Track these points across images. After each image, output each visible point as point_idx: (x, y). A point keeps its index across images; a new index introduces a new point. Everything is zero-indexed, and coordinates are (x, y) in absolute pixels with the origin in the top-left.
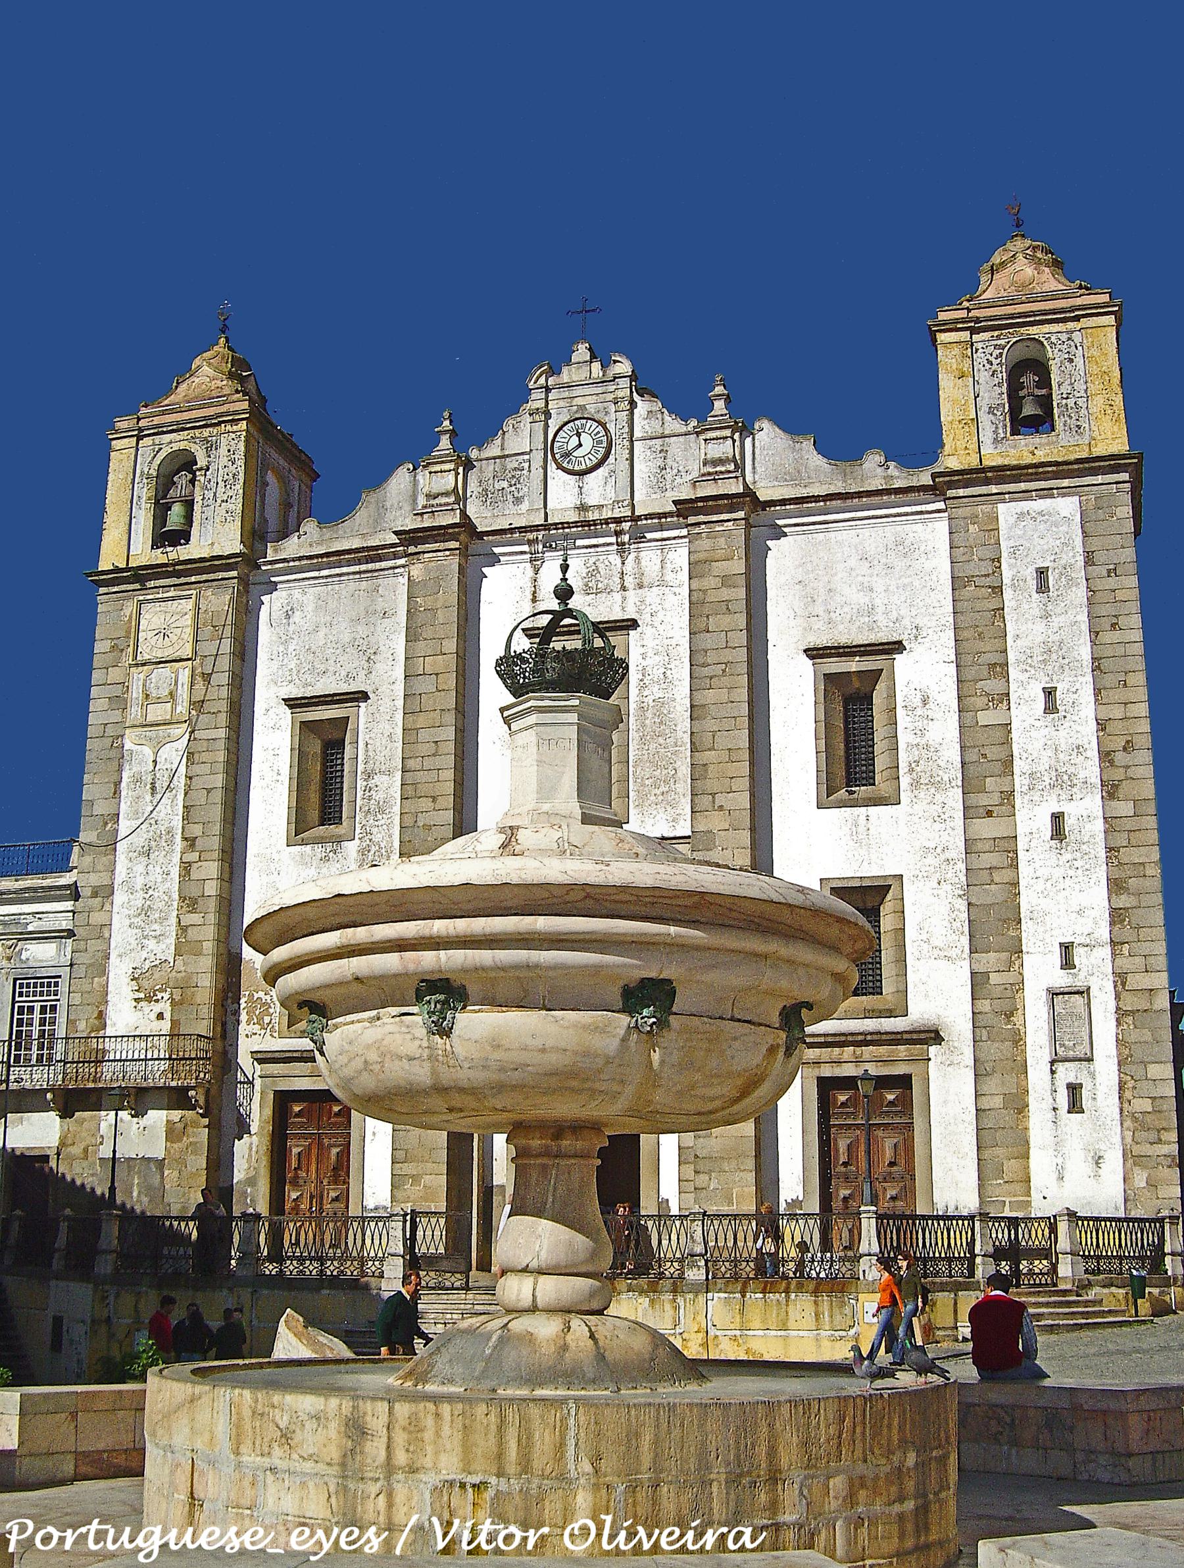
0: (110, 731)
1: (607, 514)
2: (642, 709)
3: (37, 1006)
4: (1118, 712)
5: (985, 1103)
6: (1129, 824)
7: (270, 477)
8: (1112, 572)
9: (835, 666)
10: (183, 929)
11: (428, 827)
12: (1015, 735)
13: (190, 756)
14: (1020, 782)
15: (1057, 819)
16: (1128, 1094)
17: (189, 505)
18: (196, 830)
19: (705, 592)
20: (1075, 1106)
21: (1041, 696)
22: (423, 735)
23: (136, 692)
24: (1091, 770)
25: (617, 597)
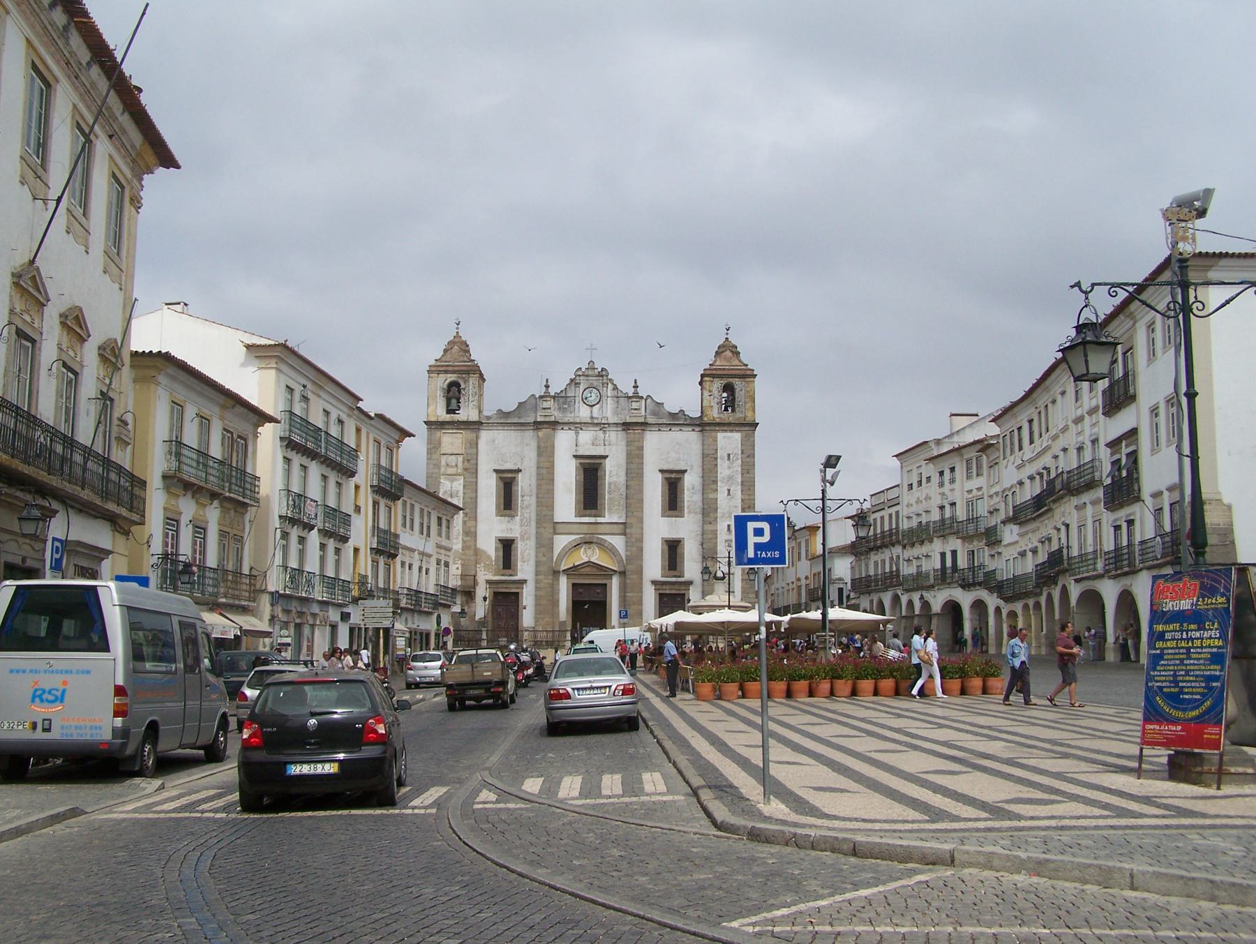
0: (434, 475)
2: (610, 484)
4: (747, 497)
8: (748, 456)
9: (667, 475)
10: (464, 542)
11: (545, 515)
13: (464, 486)
14: (719, 515)
23: (443, 463)
25: (603, 448)
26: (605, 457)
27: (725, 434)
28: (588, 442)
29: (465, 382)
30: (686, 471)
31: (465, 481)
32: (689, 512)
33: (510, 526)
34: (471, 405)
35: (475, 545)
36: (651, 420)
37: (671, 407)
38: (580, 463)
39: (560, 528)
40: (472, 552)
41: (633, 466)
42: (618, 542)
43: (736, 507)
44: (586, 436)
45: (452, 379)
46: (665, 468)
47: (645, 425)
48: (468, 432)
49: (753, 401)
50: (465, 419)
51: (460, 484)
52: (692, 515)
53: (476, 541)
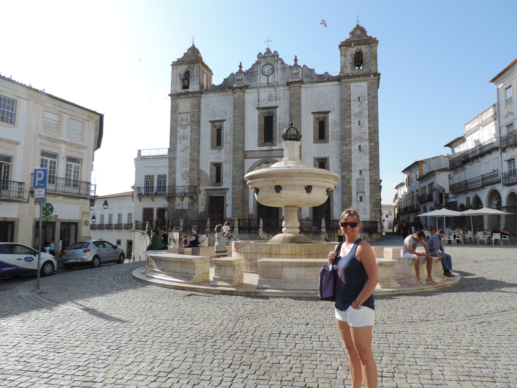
2: (279, 124)
3: (162, 180)
4: (373, 126)
5: (344, 200)
7: (204, 75)
8: (373, 97)
9: (317, 116)
10: (190, 166)
11: (238, 147)
12: (353, 131)
15: (360, 146)
16: (371, 198)
17: (189, 81)
18: (193, 146)
19: (292, 101)
20: (361, 200)
21: (358, 123)
23: (179, 119)
24: (367, 137)
25: (275, 101)
26: (276, 107)
27: (356, 84)
29: (192, 69)
30: (330, 112)
31: (191, 129)
32: (332, 139)
33: (218, 155)
34: (195, 82)
35: (198, 168)
37: (319, 71)
38: (261, 113)
39: (249, 155)
43: (365, 133)
44: (264, 94)
46: (316, 111)
49: (376, 59)
50: (192, 91)
51: (188, 131)
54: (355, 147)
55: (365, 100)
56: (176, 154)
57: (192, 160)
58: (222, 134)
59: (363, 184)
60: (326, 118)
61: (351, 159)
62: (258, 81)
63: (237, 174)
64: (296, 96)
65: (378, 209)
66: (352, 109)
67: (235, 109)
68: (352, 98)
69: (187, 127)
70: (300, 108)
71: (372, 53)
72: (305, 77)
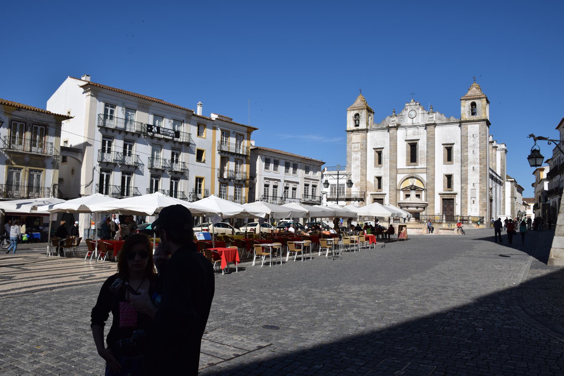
0: (350, 152)
1: (416, 124)
2: (421, 151)
4: (482, 154)
6: (483, 168)
8: (483, 135)
9: (446, 146)
10: (361, 178)
13: (361, 155)
14: (469, 163)
15: (473, 167)
17: (359, 121)
18: (362, 165)
22: (392, 154)
23: (353, 147)
24: (478, 161)
25: (417, 136)
26: (418, 140)
27: (471, 126)
28: (411, 134)
32: (456, 162)
33: (380, 171)
35: (366, 180)
36: (437, 122)
38: (408, 143)
40: (364, 182)
41: (429, 143)
42: (424, 177)
43: (477, 158)
44: (410, 131)
45: (356, 112)
46: (445, 143)
47: (435, 125)
48: (362, 133)
52: (457, 163)
53: (366, 178)
54: (470, 168)
55: (478, 136)
56: (351, 170)
57: (362, 175)
58: (382, 157)
59: (475, 193)
60: (451, 147)
61: (468, 175)
62: (406, 122)
63: (392, 184)
64: (431, 133)
65: (485, 209)
66: (469, 142)
67: (390, 141)
68: (469, 135)
69: (358, 152)
70: (434, 141)
71: (482, 105)
72: (438, 120)
